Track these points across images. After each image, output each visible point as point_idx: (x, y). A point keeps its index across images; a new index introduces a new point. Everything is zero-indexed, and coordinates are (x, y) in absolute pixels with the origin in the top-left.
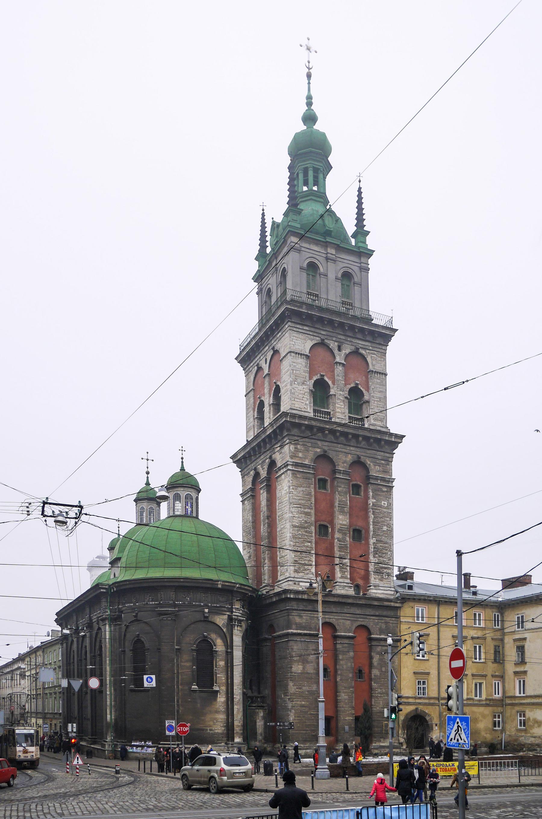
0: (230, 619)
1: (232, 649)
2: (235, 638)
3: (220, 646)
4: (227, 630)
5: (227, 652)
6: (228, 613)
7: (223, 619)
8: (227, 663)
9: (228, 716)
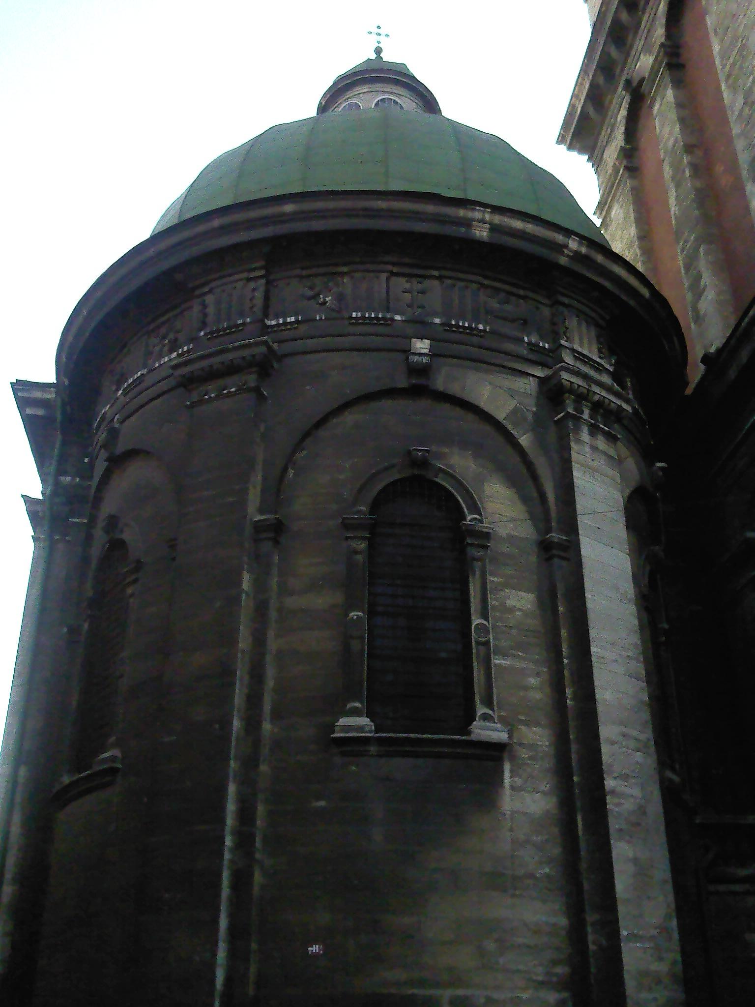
0: (552, 394)
1: (570, 525)
2: (579, 476)
3: (501, 509)
4: (541, 442)
5: (545, 547)
6: (539, 372)
7: (512, 393)
8: (547, 600)
9: (576, 910)
